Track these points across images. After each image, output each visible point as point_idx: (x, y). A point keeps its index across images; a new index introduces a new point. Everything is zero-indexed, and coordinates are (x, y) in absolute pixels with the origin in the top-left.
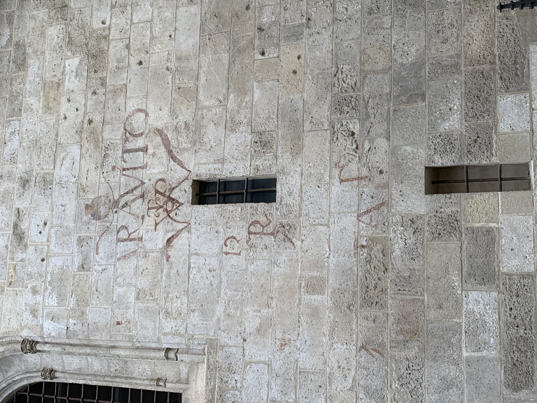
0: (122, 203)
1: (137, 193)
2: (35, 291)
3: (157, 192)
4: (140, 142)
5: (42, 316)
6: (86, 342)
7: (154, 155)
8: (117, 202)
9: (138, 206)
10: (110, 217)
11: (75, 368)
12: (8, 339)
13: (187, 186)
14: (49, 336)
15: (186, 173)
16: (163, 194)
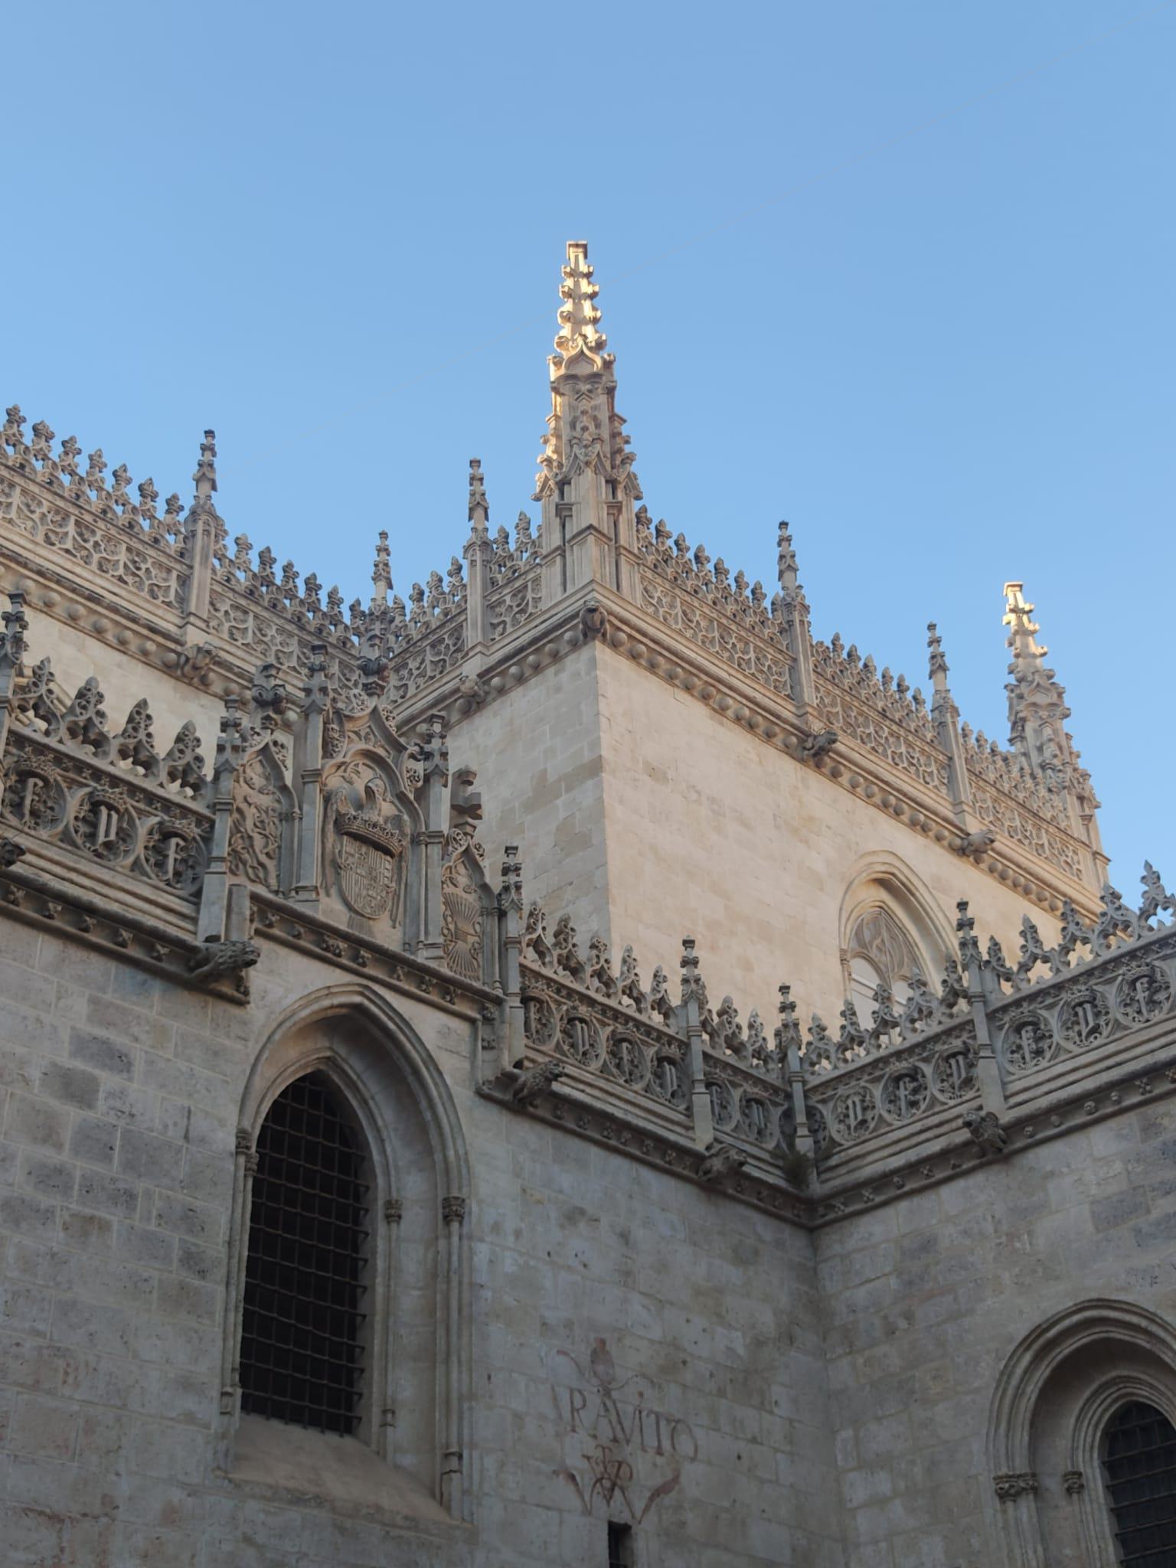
0: (609, 1403)
1: (620, 1435)
2: (518, 1234)
3: (620, 1464)
4: (666, 1444)
5: (492, 1243)
6: (465, 1312)
7: (655, 1465)
8: (607, 1393)
9: (605, 1432)
10: (595, 1381)
11: (399, 1259)
12: (464, 1171)
13: (623, 1518)
14: (472, 1253)
15: (638, 1515)
16: (617, 1475)
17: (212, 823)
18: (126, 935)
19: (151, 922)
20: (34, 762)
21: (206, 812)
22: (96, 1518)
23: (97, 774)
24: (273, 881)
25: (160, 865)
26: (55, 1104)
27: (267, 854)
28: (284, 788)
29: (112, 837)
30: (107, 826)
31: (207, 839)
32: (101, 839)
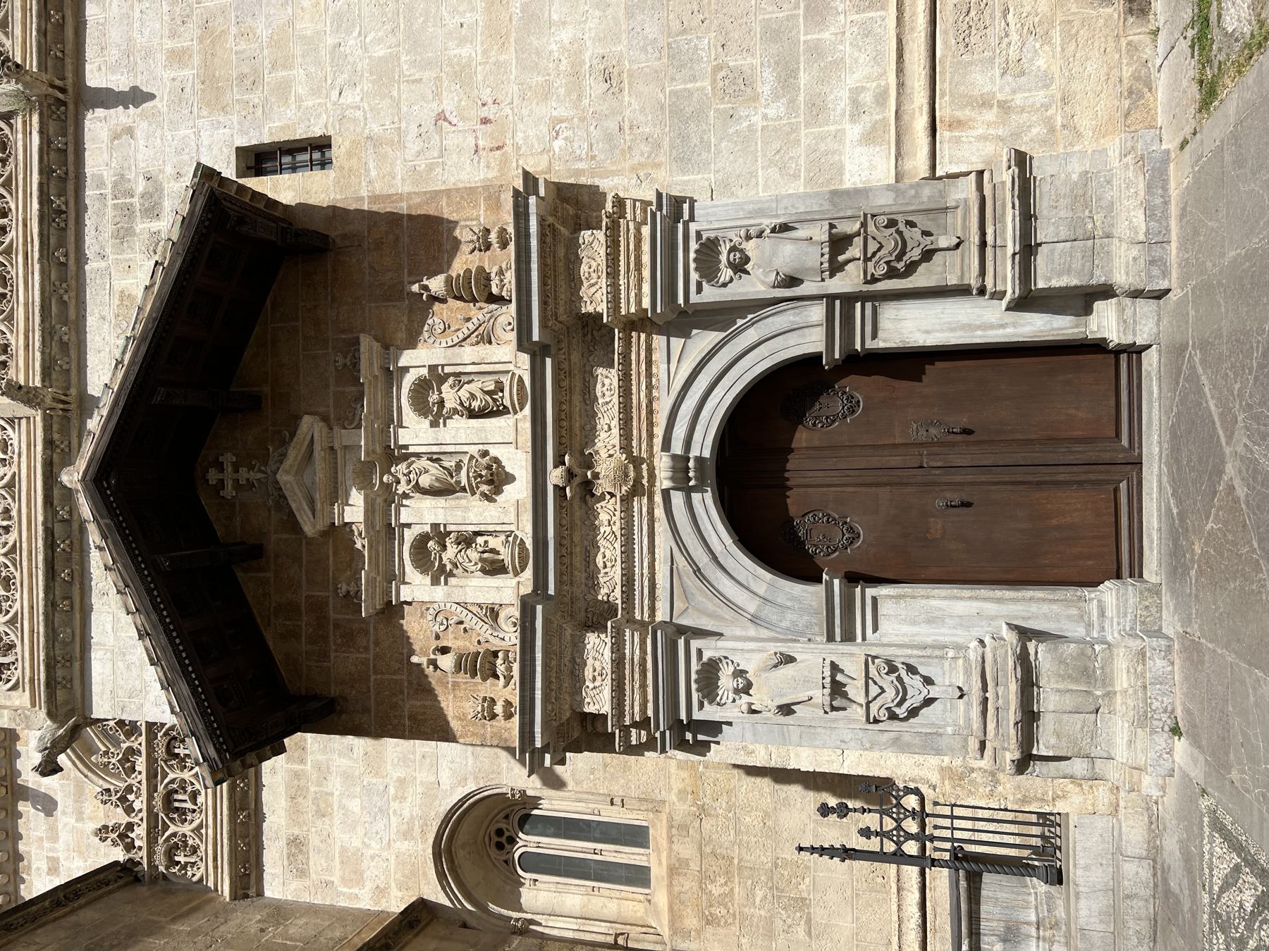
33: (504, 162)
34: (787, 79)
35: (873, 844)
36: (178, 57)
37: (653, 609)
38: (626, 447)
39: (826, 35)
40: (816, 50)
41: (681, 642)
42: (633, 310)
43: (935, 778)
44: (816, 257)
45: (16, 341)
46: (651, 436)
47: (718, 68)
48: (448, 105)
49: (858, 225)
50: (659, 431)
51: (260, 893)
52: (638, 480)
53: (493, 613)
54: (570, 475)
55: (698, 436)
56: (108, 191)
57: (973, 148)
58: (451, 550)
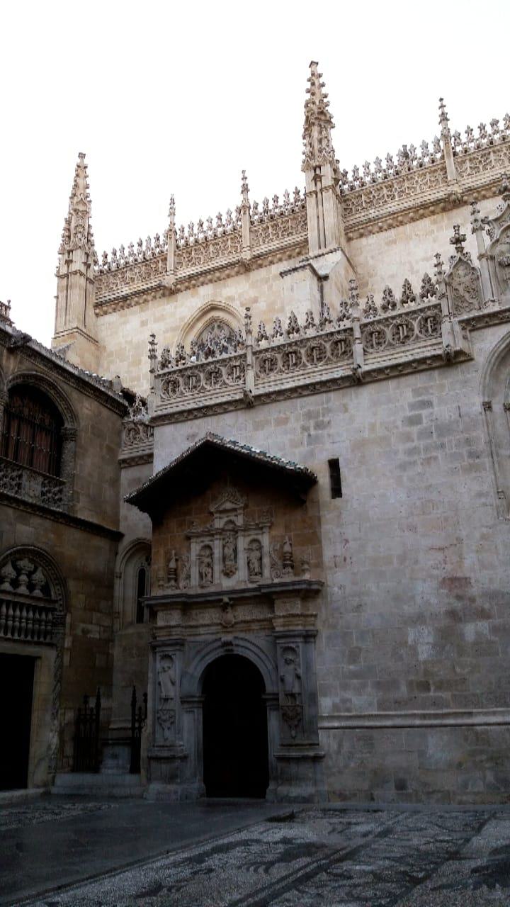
17: (440, 305)
18: (414, 365)
19: (417, 357)
20: (370, 328)
21: (438, 302)
22: (456, 545)
23: (393, 318)
24: (477, 306)
25: (427, 331)
26: (408, 429)
27: (472, 298)
28: (473, 268)
29: (405, 334)
30: (403, 332)
31: (441, 311)
32: (402, 337)
33: (331, 568)
34: (355, 675)
35: (137, 712)
36: (372, 427)
37: (190, 635)
38: (236, 623)
39: (369, 689)
40: (364, 686)
41: (178, 647)
42: (275, 624)
43: (148, 731)
44: (288, 688)
45: (273, 376)
46: (242, 631)
47: (360, 649)
48: (352, 544)
49: (297, 703)
50: (242, 635)
51: (122, 468)
52: (226, 627)
53: (188, 577)
54: (227, 604)
55: (240, 649)
56: (325, 406)
57: (327, 741)
58: (207, 560)
